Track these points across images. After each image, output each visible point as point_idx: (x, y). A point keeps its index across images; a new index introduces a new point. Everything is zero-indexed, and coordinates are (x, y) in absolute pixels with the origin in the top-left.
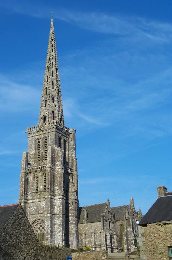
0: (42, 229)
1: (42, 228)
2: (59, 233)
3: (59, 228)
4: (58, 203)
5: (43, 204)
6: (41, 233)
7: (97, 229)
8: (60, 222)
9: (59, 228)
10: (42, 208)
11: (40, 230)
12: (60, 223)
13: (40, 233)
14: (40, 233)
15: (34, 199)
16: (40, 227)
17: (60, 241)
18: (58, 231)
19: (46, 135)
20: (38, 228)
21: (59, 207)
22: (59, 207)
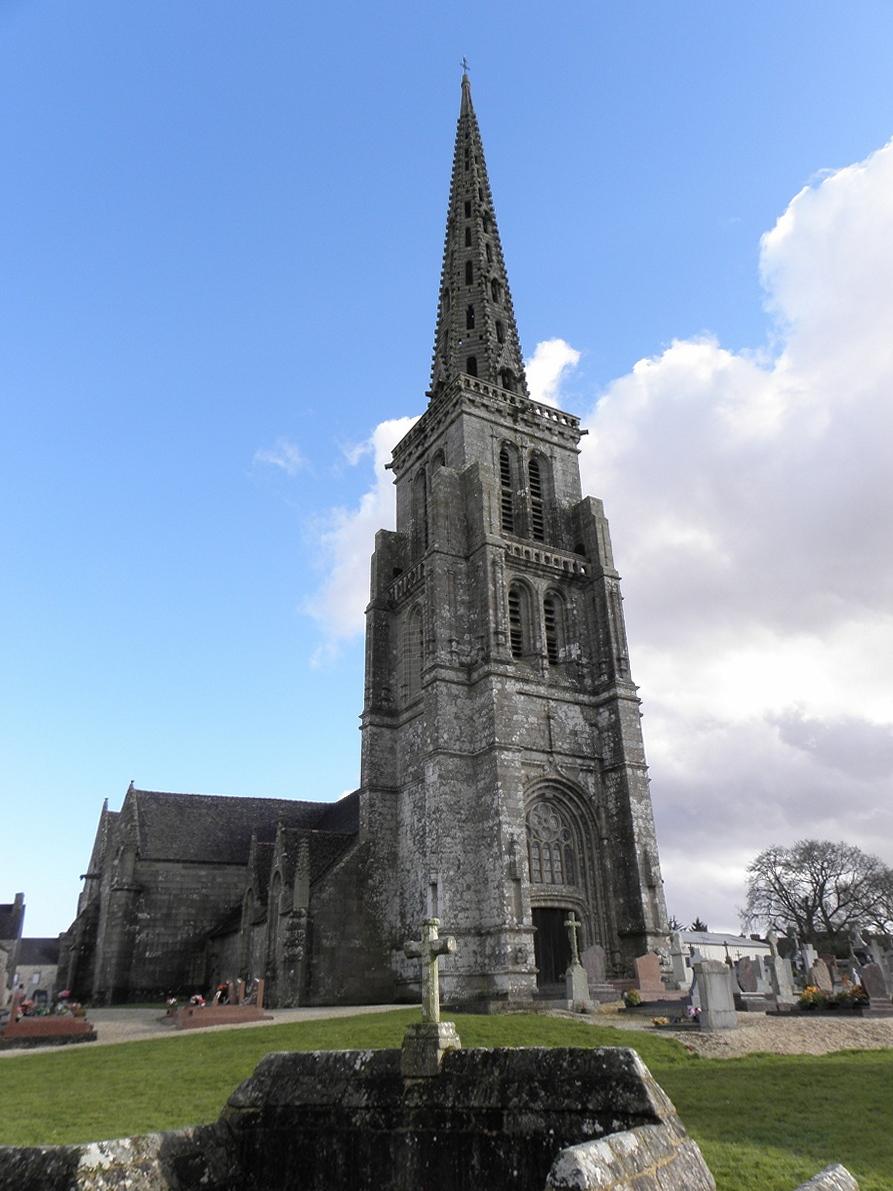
5: (570, 714)
10: (568, 731)
19: (543, 448)
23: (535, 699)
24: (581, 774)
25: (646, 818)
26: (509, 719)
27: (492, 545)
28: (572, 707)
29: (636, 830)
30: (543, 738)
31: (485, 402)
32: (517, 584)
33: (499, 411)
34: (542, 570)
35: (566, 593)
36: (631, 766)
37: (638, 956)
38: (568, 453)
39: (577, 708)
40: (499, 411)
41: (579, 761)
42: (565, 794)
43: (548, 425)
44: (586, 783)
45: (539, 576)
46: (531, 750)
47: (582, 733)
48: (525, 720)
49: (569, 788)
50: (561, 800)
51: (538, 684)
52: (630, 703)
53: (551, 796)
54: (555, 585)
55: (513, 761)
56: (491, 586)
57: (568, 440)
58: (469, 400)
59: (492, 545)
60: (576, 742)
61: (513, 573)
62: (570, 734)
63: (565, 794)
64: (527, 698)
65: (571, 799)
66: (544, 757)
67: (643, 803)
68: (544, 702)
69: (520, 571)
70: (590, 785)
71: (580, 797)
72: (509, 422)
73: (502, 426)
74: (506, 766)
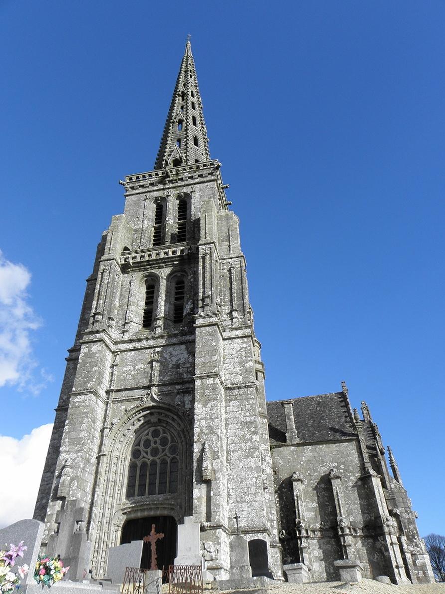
0: (160, 447)
1: (159, 442)
2: (247, 457)
3: (247, 437)
4: (237, 351)
5: (174, 353)
6: (154, 463)
7: (344, 463)
8: (247, 414)
9: (247, 437)
10: (170, 366)
11: (149, 451)
12: (248, 419)
13: (149, 463)
14: (149, 463)
15: (138, 340)
16: (150, 437)
17: (253, 491)
18: (241, 449)
19: (185, 190)
20: (142, 443)
21: (240, 363)
22: (240, 363)
23: (144, 350)
24: (178, 397)
25: (211, 418)
26: (88, 372)
27: (104, 261)
28: (177, 347)
29: (197, 430)
30: (146, 377)
31: (141, 184)
32: (150, 279)
33: (152, 184)
34: (160, 263)
35: (187, 270)
36: (200, 377)
37: (323, 552)
38: (206, 184)
39: (183, 347)
40: (152, 184)
41: (178, 387)
42: (167, 416)
43: (190, 175)
44: (183, 403)
45: (163, 267)
46: (132, 389)
47: (184, 364)
48: (132, 368)
49: (169, 410)
50: (168, 422)
51: (148, 339)
52: (208, 328)
53: (157, 420)
54: (178, 268)
55: (84, 401)
56: (98, 286)
57: (207, 176)
58: (131, 187)
59: (104, 261)
60: (178, 373)
61: (142, 273)
62: (173, 367)
63: (167, 416)
64: (137, 351)
65: (173, 420)
66: (143, 392)
67: (209, 405)
68: (152, 350)
69: (146, 270)
70: (186, 403)
71: (178, 416)
72: (161, 186)
73: (154, 191)
74: (76, 407)
